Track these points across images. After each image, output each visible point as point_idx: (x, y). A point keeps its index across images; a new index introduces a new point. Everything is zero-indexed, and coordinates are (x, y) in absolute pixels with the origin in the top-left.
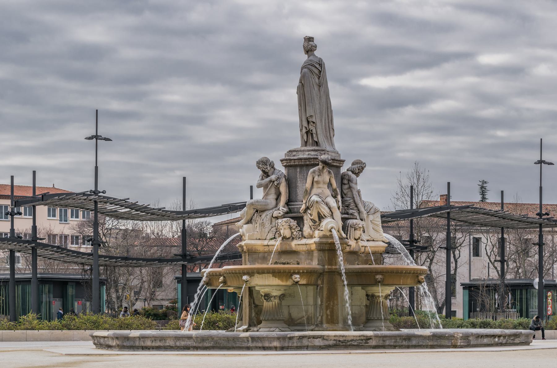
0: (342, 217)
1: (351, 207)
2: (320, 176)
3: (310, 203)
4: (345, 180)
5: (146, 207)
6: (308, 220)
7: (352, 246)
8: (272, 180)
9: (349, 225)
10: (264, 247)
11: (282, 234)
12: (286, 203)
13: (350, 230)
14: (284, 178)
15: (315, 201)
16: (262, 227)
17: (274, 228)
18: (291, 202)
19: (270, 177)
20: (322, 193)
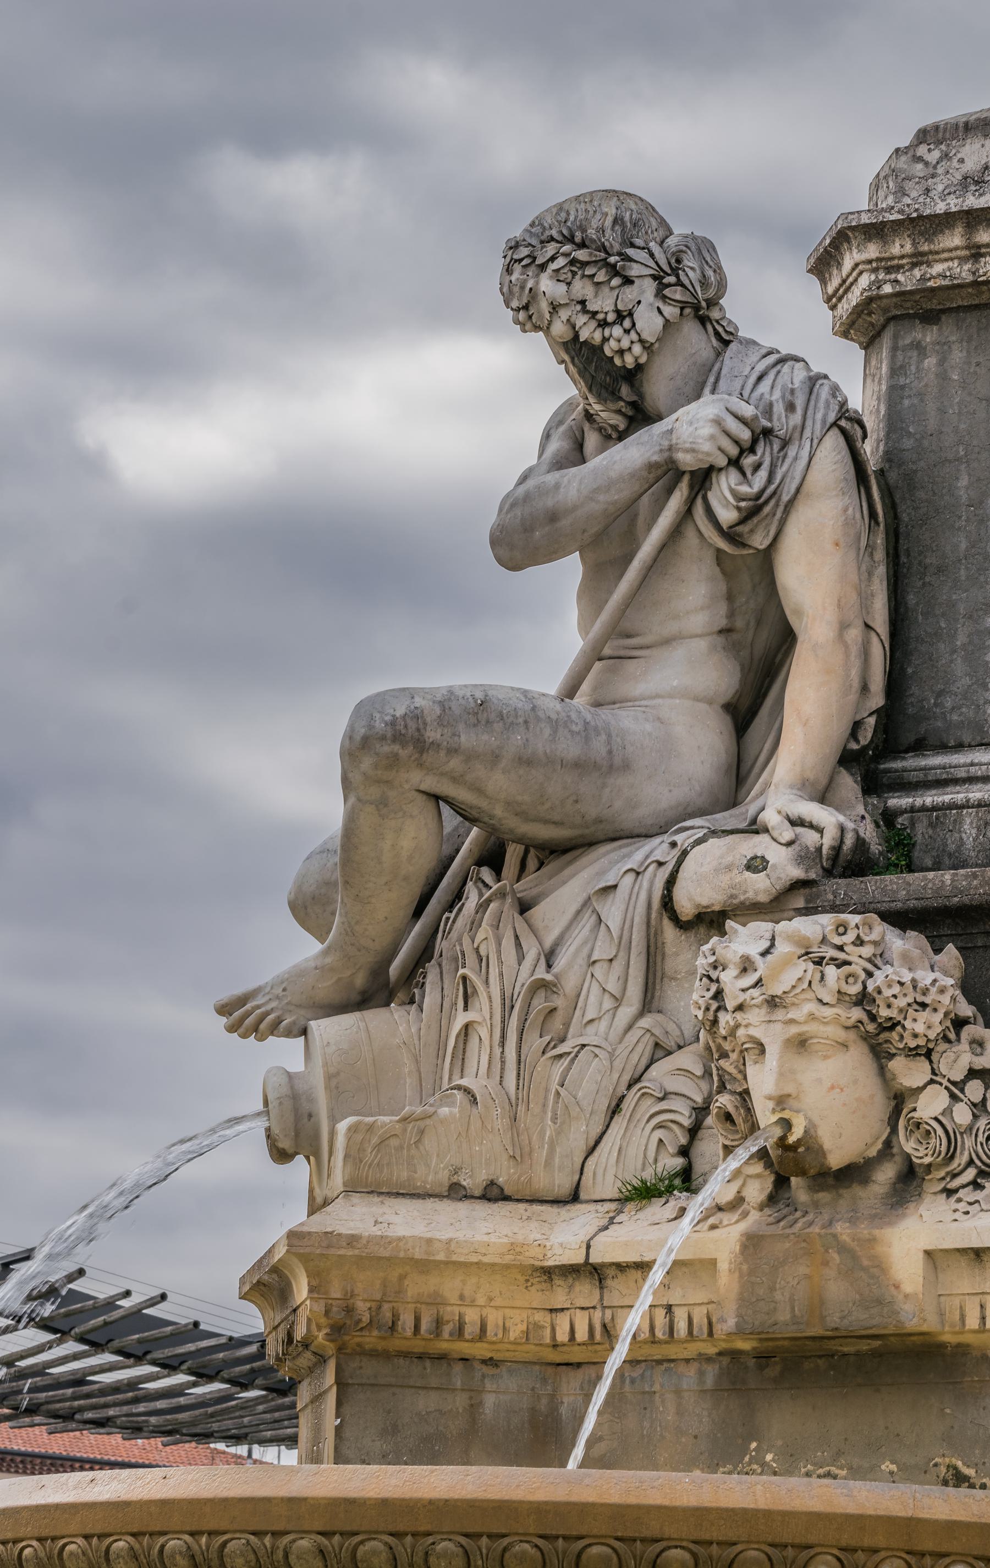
5: (137, 1318)
8: (686, 460)
10: (537, 1296)
11: (766, 1116)
12: (847, 759)
14: (834, 441)
16: (535, 1042)
17: (688, 1059)
18: (919, 746)
19: (658, 428)
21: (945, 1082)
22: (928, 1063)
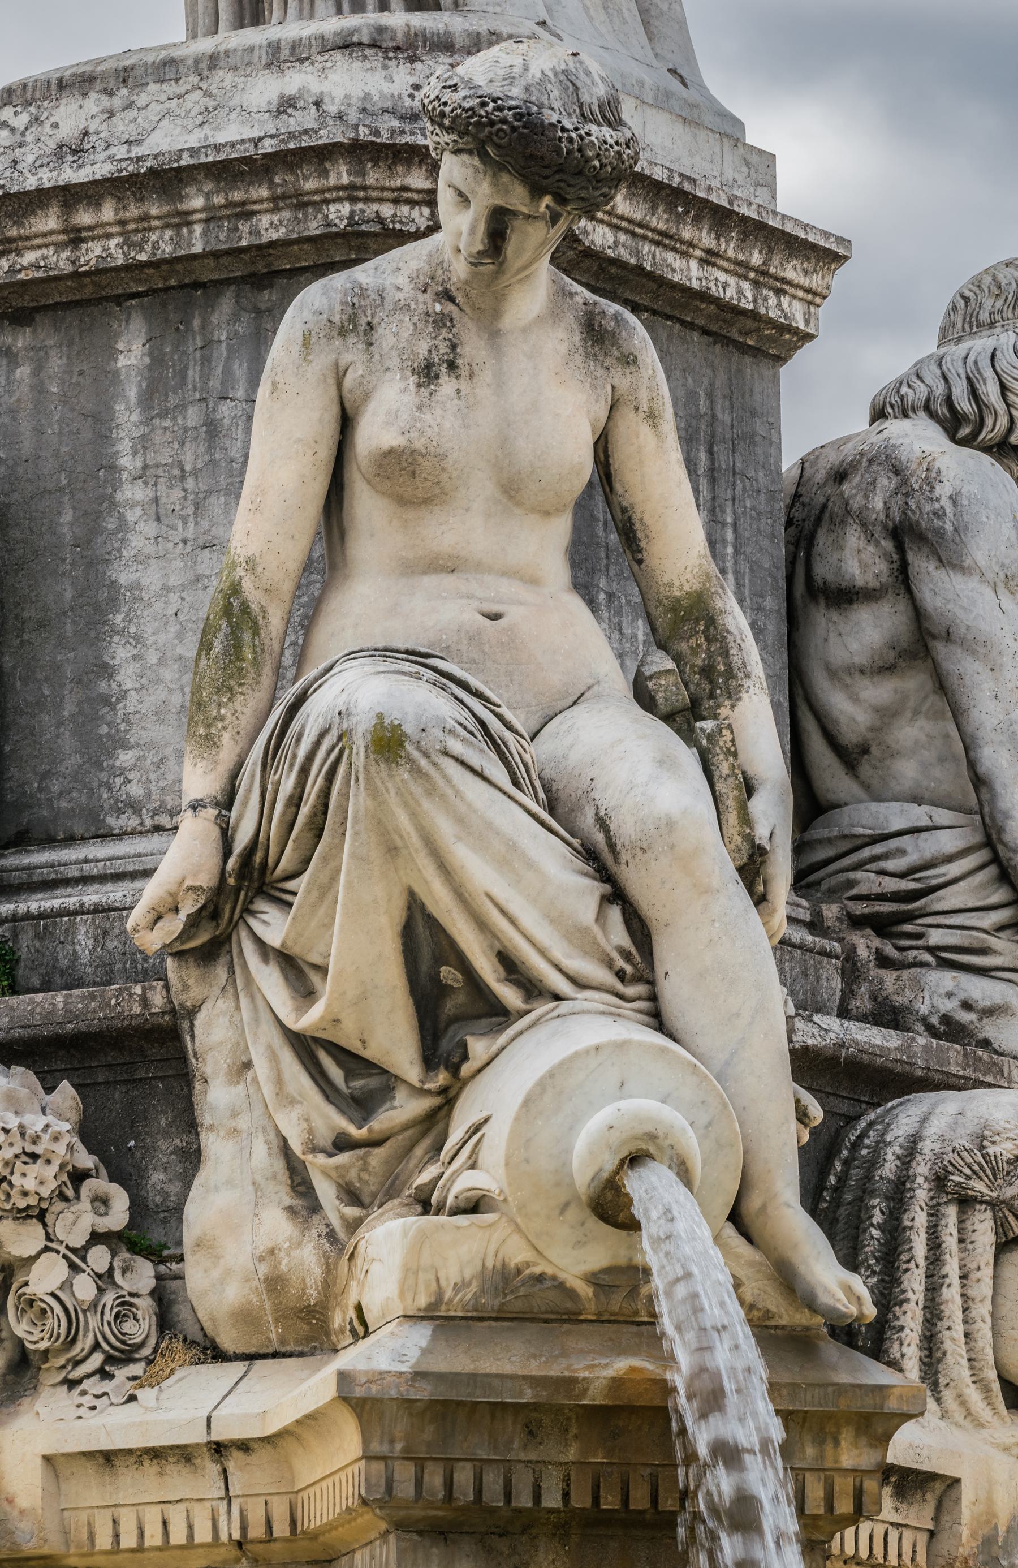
0: (808, 1035)
1: (936, 937)
2: (447, 386)
3: (288, 785)
4: (853, 537)
6: (261, 1068)
7: (967, 1493)
9: (921, 1169)
13: (935, 1245)
15: (362, 725)
18: (22, 841)
20: (474, 637)
21: (63, 1250)
22: (40, 1227)
